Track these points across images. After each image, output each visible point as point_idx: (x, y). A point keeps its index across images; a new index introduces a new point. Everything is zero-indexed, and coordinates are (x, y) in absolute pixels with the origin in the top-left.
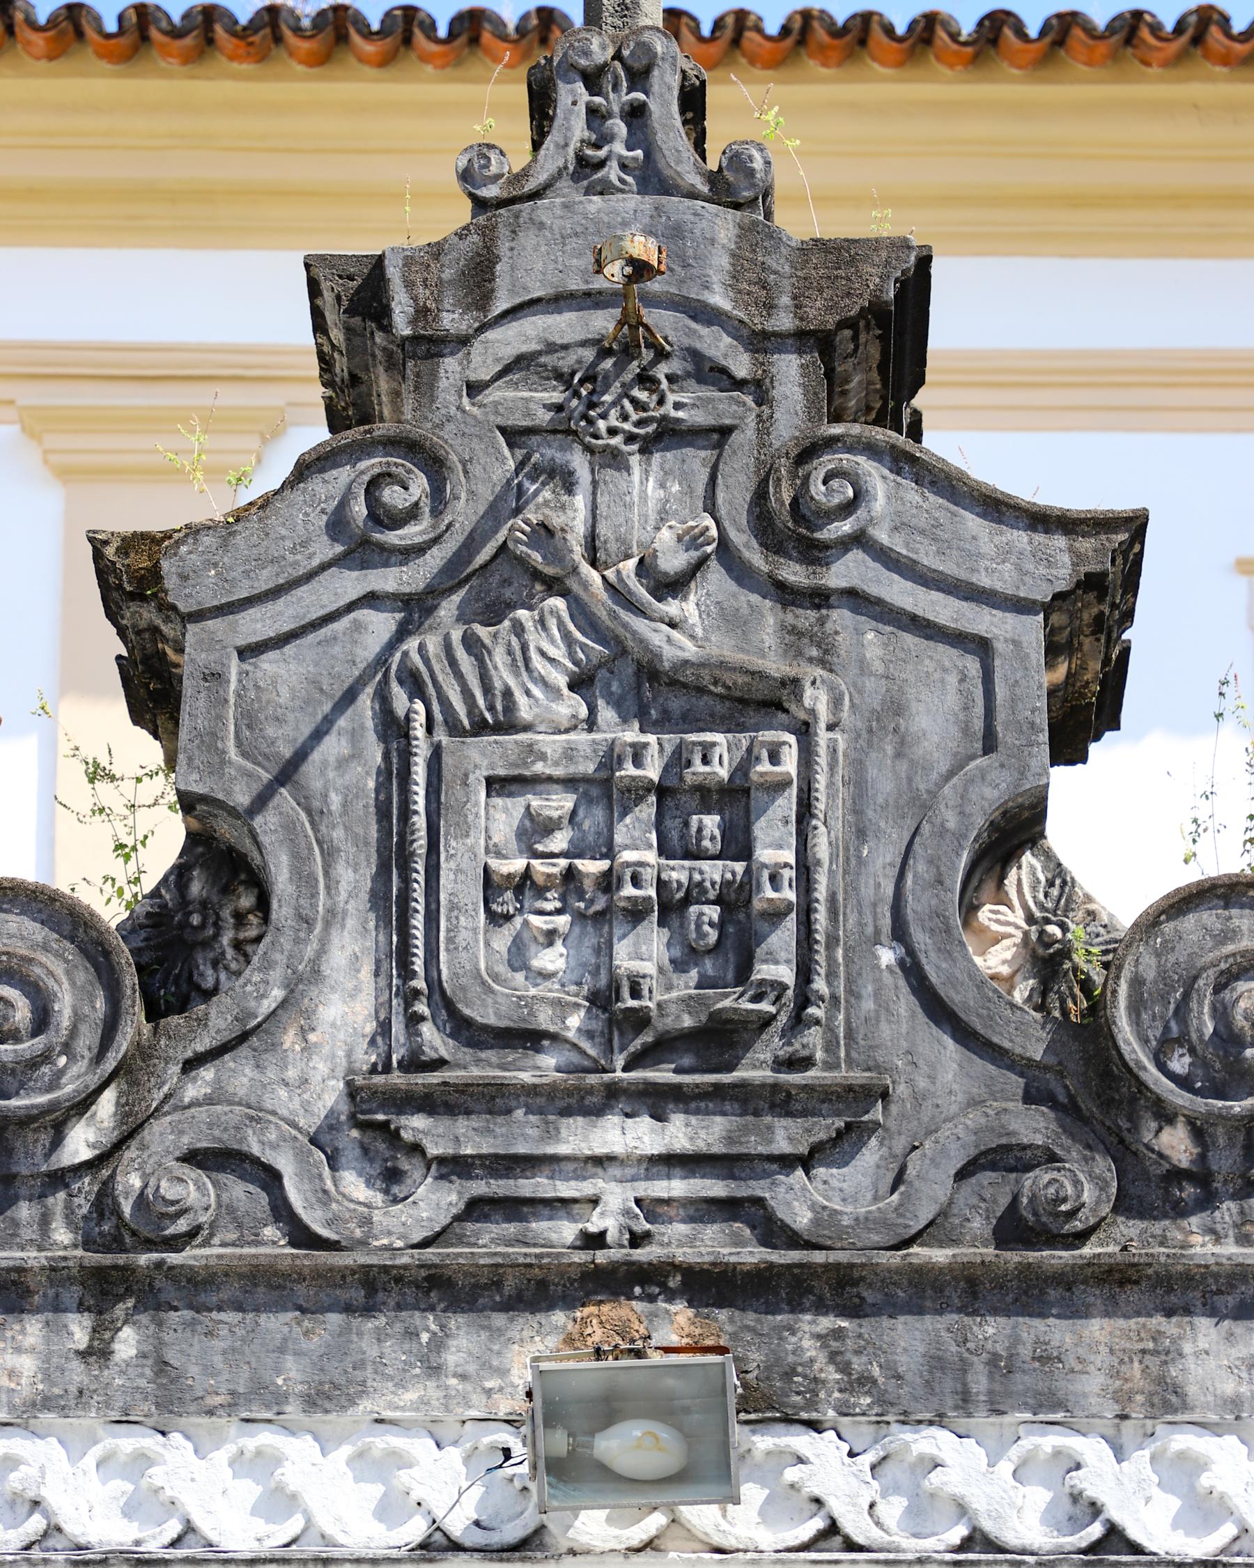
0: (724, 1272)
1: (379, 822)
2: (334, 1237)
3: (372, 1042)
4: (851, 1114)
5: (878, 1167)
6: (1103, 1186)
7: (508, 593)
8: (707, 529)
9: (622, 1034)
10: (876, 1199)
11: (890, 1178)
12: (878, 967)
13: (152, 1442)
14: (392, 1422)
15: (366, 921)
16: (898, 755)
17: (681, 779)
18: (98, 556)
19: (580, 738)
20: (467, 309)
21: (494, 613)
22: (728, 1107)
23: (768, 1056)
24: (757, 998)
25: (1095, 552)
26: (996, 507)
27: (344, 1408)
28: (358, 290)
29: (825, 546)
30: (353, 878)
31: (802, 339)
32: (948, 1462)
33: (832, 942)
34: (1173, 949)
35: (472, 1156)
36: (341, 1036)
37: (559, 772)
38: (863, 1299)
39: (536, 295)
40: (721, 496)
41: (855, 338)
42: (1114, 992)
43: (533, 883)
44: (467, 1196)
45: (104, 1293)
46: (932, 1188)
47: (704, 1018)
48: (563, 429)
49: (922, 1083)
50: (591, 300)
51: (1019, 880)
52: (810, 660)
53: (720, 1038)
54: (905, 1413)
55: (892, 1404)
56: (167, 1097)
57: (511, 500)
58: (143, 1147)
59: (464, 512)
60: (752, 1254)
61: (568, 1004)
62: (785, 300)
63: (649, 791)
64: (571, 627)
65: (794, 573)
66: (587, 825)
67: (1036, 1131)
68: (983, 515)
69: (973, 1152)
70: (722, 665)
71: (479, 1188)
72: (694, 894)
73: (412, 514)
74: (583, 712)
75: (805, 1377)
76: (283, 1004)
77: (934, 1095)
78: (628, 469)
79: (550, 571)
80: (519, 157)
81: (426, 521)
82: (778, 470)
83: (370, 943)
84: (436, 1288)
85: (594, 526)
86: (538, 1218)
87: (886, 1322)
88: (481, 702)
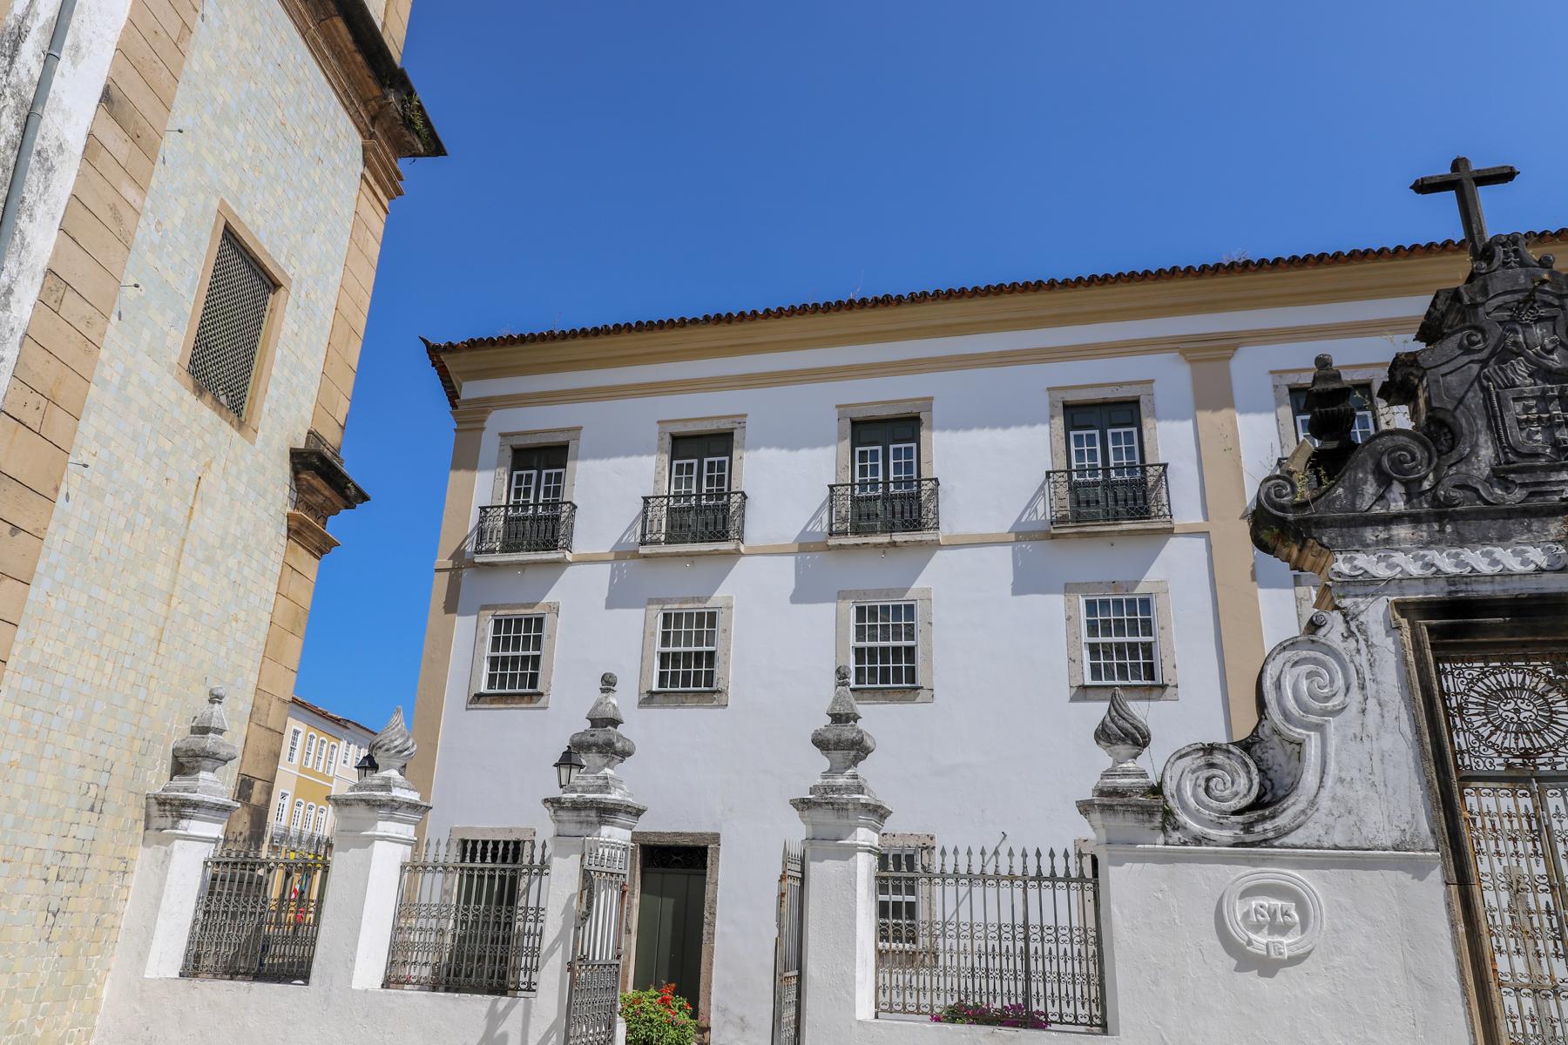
30: (1481, 423)
48: (1513, 320)
57: (1503, 338)
59: (1492, 342)
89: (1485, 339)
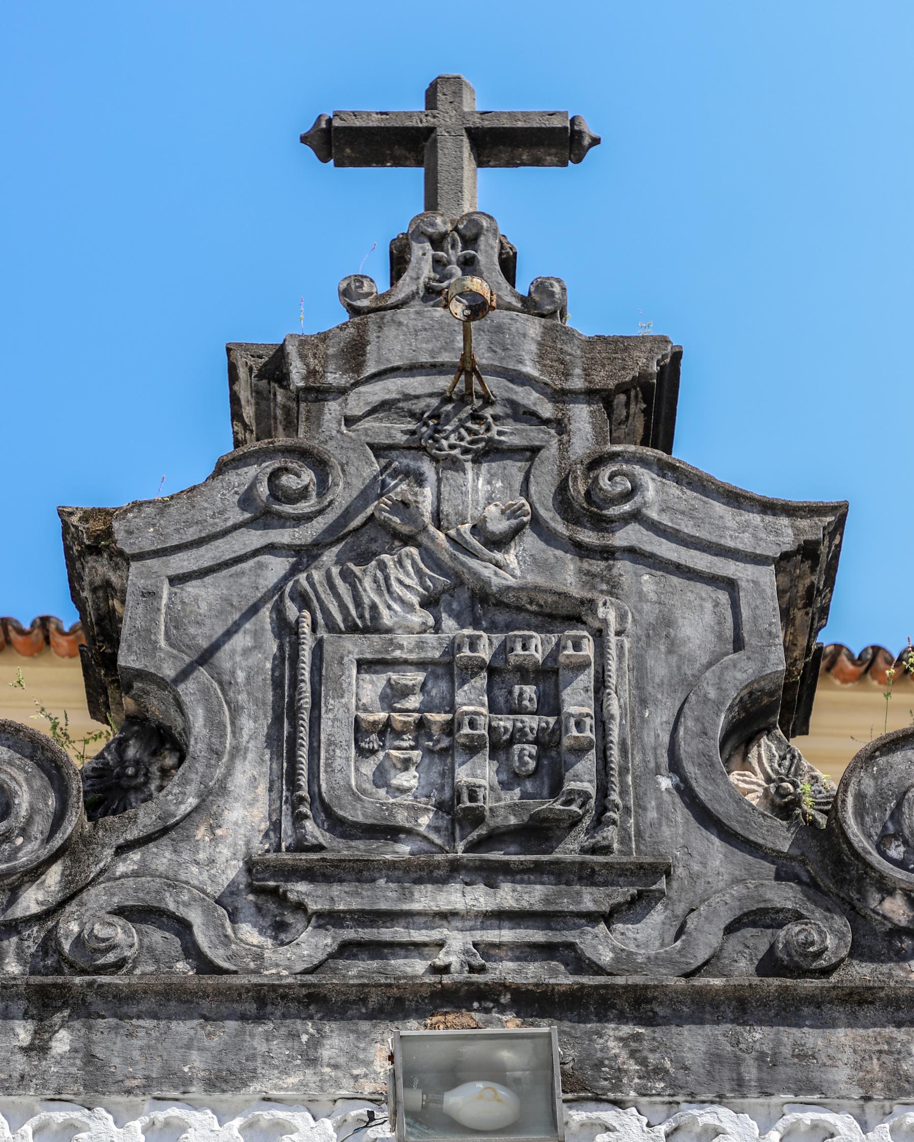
0: (545, 992)
1: (274, 690)
2: (234, 968)
3: (266, 835)
4: (644, 884)
5: (664, 923)
6: (841, 936)
7: (374, 547)
8: (523, 505)
9: (462, 828)
10: (662, 945)
11: (673, 931)
12: (659, 789)
13: (78, 1115)
14: (277, 1100)
15: (263, 754)
16: (670, 652)
17: (507, 661)
18: (66, 527)
19: (430, 637)
20: (345, 372)
21: (363, 558)
22: (545, 878)
23: (576, 846)
24: (568, 802)
25: (813, 529)
26: (735, 498)
27: (238, 1089)
28: (265, 365)
29: (610, 520)
30: (253, 727)
31: (590, 395)
32: (728, 1130)
33: (623, 771)
34: (886, 774)
35: (343, 912)
36: (242, 831)
37: (413, 657)
38: (655, 1013)
39: (396, 364)
40: (533, 489)
41: (627, 405)
42: (844, 801)
43: (393, 730)
44: (339, 940)
45: (45, 1006)
46: (706, 939)
47: (526, 818)
49: (696, 867)
50: (436, 369)
51: (759, 755)
52: (602, 592)
53: (538, 832)
54: (692, 1094)
55: (681, 1088)
56: (102, 872)
57: (375, 489)
58: (82, 904)
59: (342, 495)
60: (565, 980)
61: (419, 809)
62: (578, 371)
63: (482, 669)
64: (422, 566)
65: (588, 537)
66: (434, 692)
67: (787, 899)
68: (727, 504)
69: (738, 913)
70: (537, 588)
71: (350, 934)
72: (517, 736)
73: (303, 494)
74: (431, 621)
75: (611, 1068)
76: (196, 809)
77: (705, 875)
78: (464, 471)
79: (405, 529)
80: (382, 285)
81: (313, 499)
82: (575, 472)
83: (266, 769)
84: (313, 1001)
85: (438, 506)
86: (396, 957)
87: (674, 1029)
88: (353, 612)
89: (323, 485)
